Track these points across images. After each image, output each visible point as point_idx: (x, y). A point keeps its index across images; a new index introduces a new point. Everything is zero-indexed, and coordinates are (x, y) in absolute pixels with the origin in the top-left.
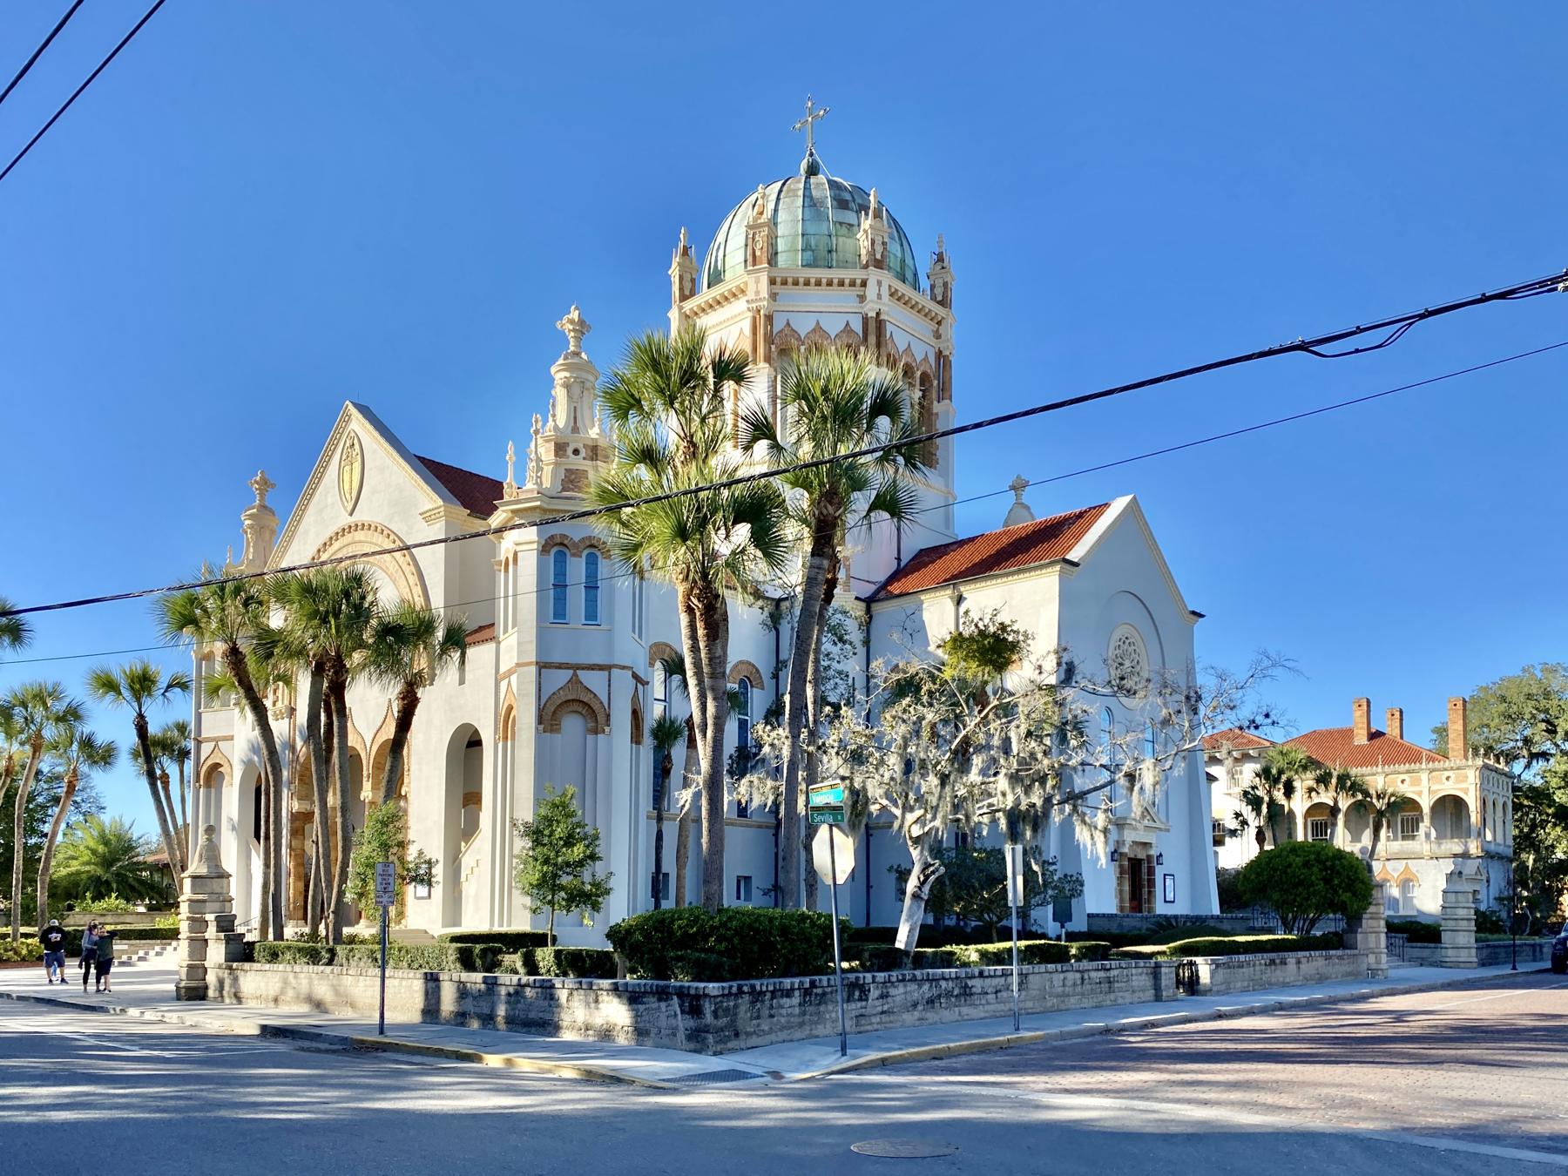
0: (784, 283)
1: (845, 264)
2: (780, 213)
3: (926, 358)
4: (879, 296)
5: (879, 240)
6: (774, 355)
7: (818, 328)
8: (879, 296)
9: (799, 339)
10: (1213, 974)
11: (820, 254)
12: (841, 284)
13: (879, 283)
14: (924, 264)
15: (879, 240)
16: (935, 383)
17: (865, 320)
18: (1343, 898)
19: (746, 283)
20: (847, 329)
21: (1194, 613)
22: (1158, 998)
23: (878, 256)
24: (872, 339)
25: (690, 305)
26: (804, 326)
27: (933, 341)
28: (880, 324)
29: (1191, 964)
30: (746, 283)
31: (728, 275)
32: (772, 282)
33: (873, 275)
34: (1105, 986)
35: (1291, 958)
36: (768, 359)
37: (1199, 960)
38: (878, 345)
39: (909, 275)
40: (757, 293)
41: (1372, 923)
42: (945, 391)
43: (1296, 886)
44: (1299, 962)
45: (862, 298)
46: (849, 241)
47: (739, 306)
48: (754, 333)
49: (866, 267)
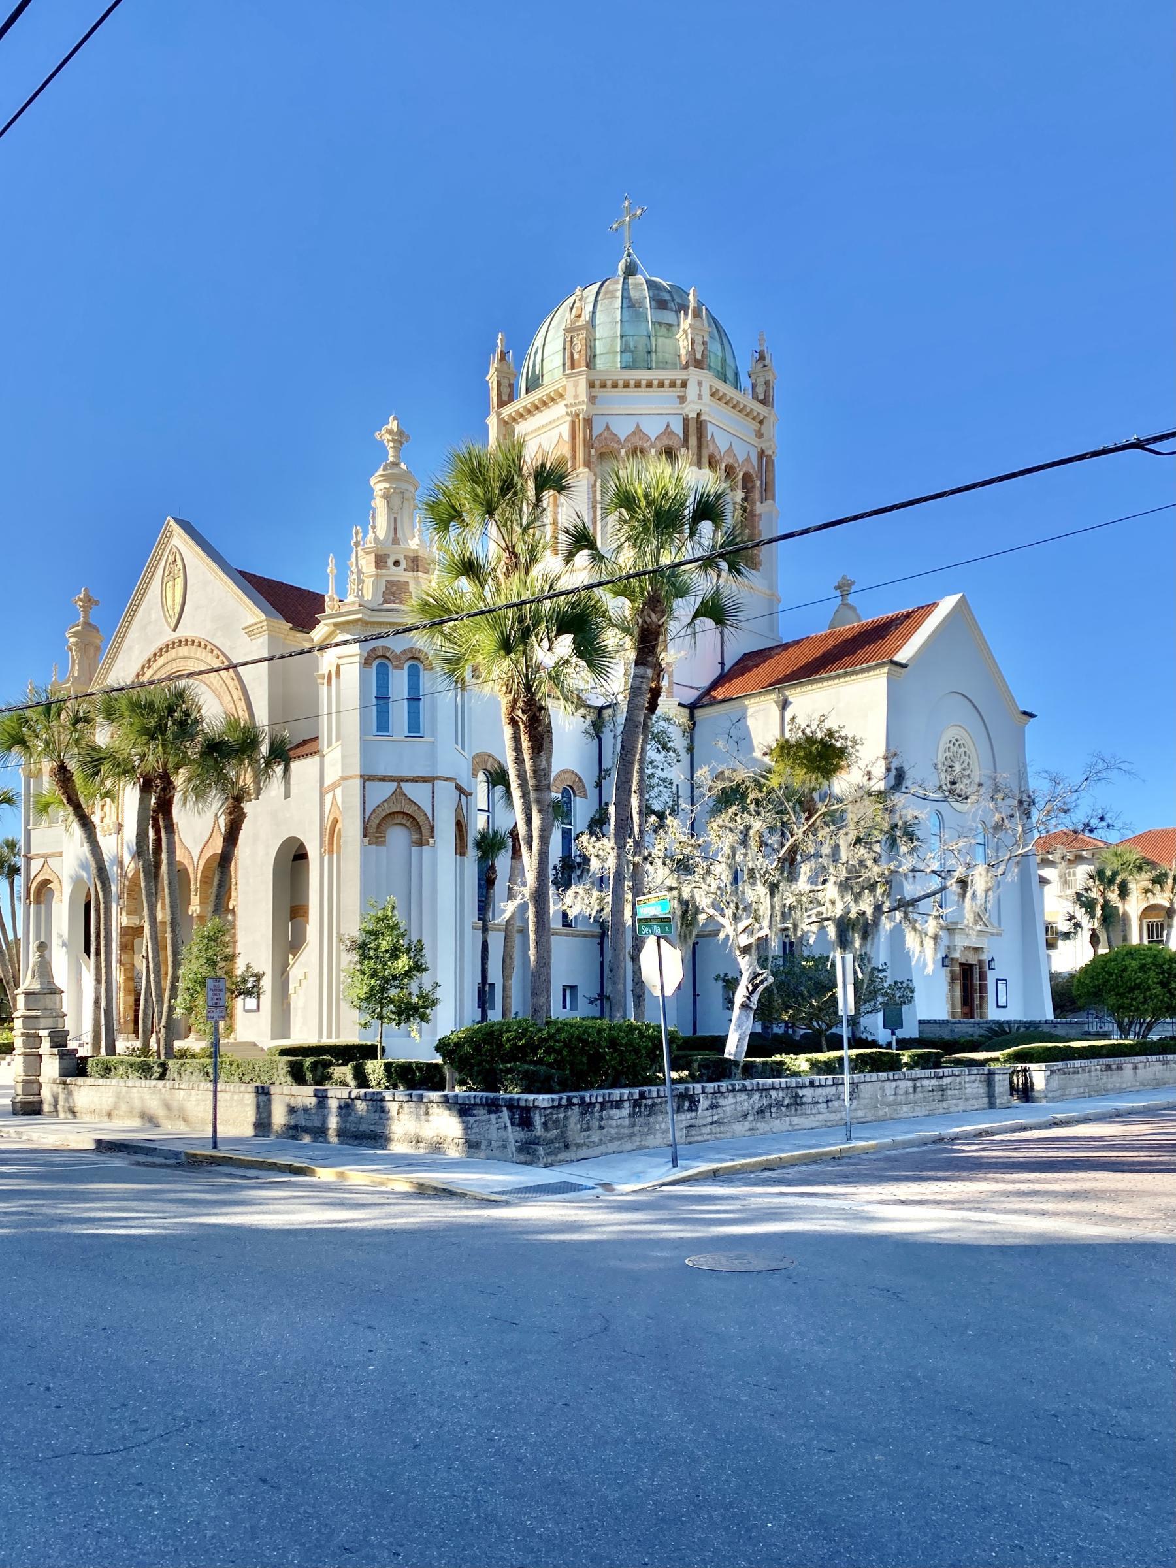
0: (604, 386)
1: (664, 365)
2: (598, 315)
3: (748, 459)
4: (700, 397)
5: (699, 340)
6: (594, 460)
7: (638, 431)
8: (700, 397)
9: (619, 442)
10: (1047, 1080)
11: (638, 356)
12: (661, 385)
13: (700, 383)
14: (745, 363)
15: (699, 340)
16: (758, 483)
17: (686, 422)
19: (564, 387)
20: (668, 431)
22: (992, 1105)
23: (699, 356)
24: (693, 441)
25: (508, 411)
26: (623, 430)
28: (701, 425)
29: (1025, 1070)
30: (564, 387)
31: (546, 380)
32: (591, 385)
33: (693, 375)
34: (938, 1094)
35: (1128, 1062)
36: (587, 464)
37: (1032, 1066)
38: (700, 446)
39: (730, 375)
40: (576, 396)
42: (767, 491)
44: (1135, 1068)
45: (683, 399)
46: (667, 341)
47: (558, 410)
48: (573, 436)
49: (686, 367)
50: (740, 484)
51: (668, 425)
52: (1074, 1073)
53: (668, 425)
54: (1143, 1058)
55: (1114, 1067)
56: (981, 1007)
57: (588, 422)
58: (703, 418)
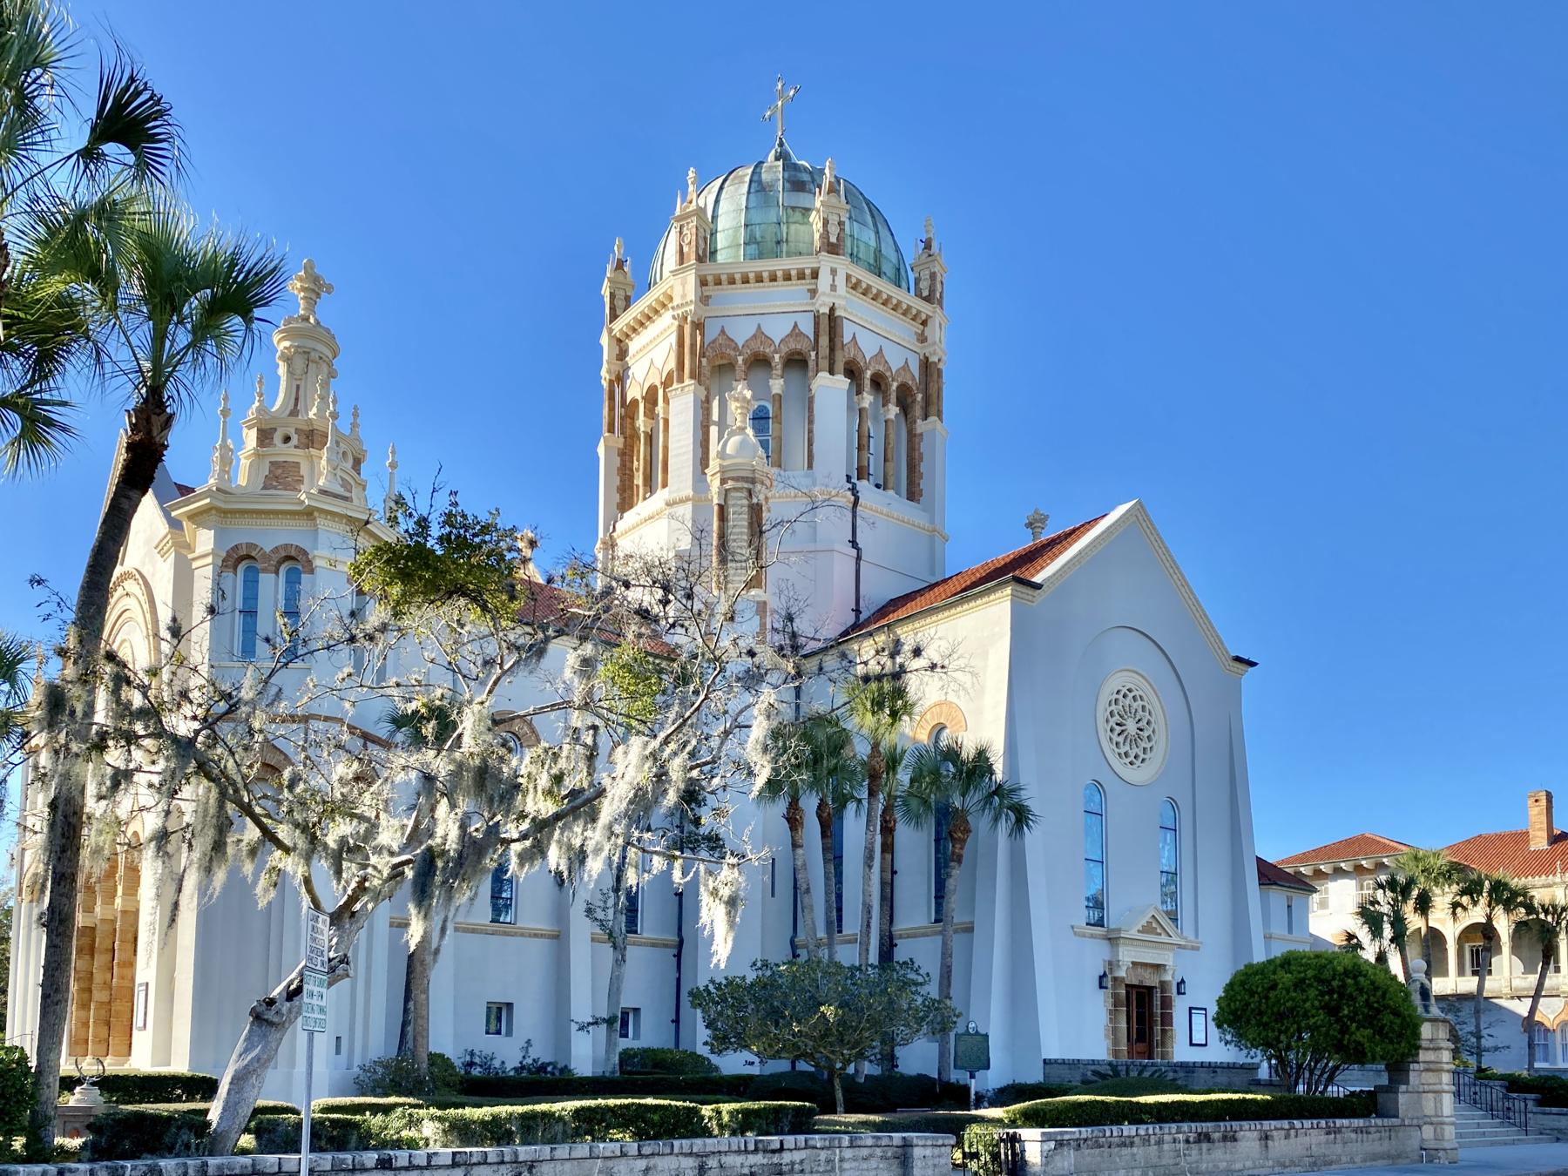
7: (759, 334)
9: (736, 348)
10: (1047, 1157)
16: (919, 397)
17: (817, 319)
18: (1358, 1036)
20: (796, 332)
21: (1238, 659)
24: (824, 341)
27: (917, 346)
29: (1014, 1139)
35: (1248, 1133)
38: (832, 349)
41: (1428, 1077)
43: (1280, 1017)
44: (1266, 1137)
50: (893, 397)
51: (796, 325)
52: (1123, 1145)
53: (796, 325)
54: (1285, 1124)
55: (1216, 1136)
56: (1163, 1044)
57: (698, 326)
58: (838, 313)
